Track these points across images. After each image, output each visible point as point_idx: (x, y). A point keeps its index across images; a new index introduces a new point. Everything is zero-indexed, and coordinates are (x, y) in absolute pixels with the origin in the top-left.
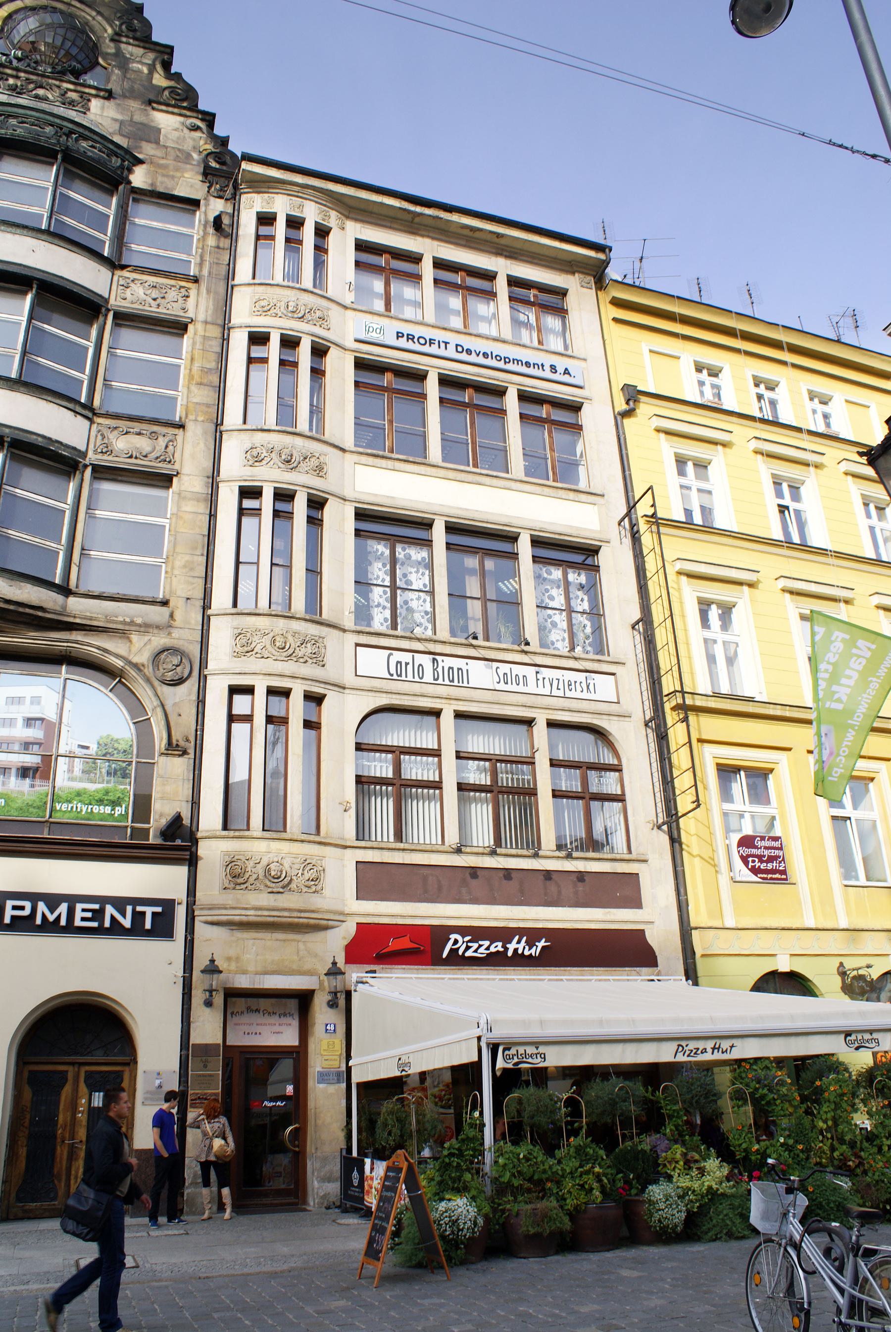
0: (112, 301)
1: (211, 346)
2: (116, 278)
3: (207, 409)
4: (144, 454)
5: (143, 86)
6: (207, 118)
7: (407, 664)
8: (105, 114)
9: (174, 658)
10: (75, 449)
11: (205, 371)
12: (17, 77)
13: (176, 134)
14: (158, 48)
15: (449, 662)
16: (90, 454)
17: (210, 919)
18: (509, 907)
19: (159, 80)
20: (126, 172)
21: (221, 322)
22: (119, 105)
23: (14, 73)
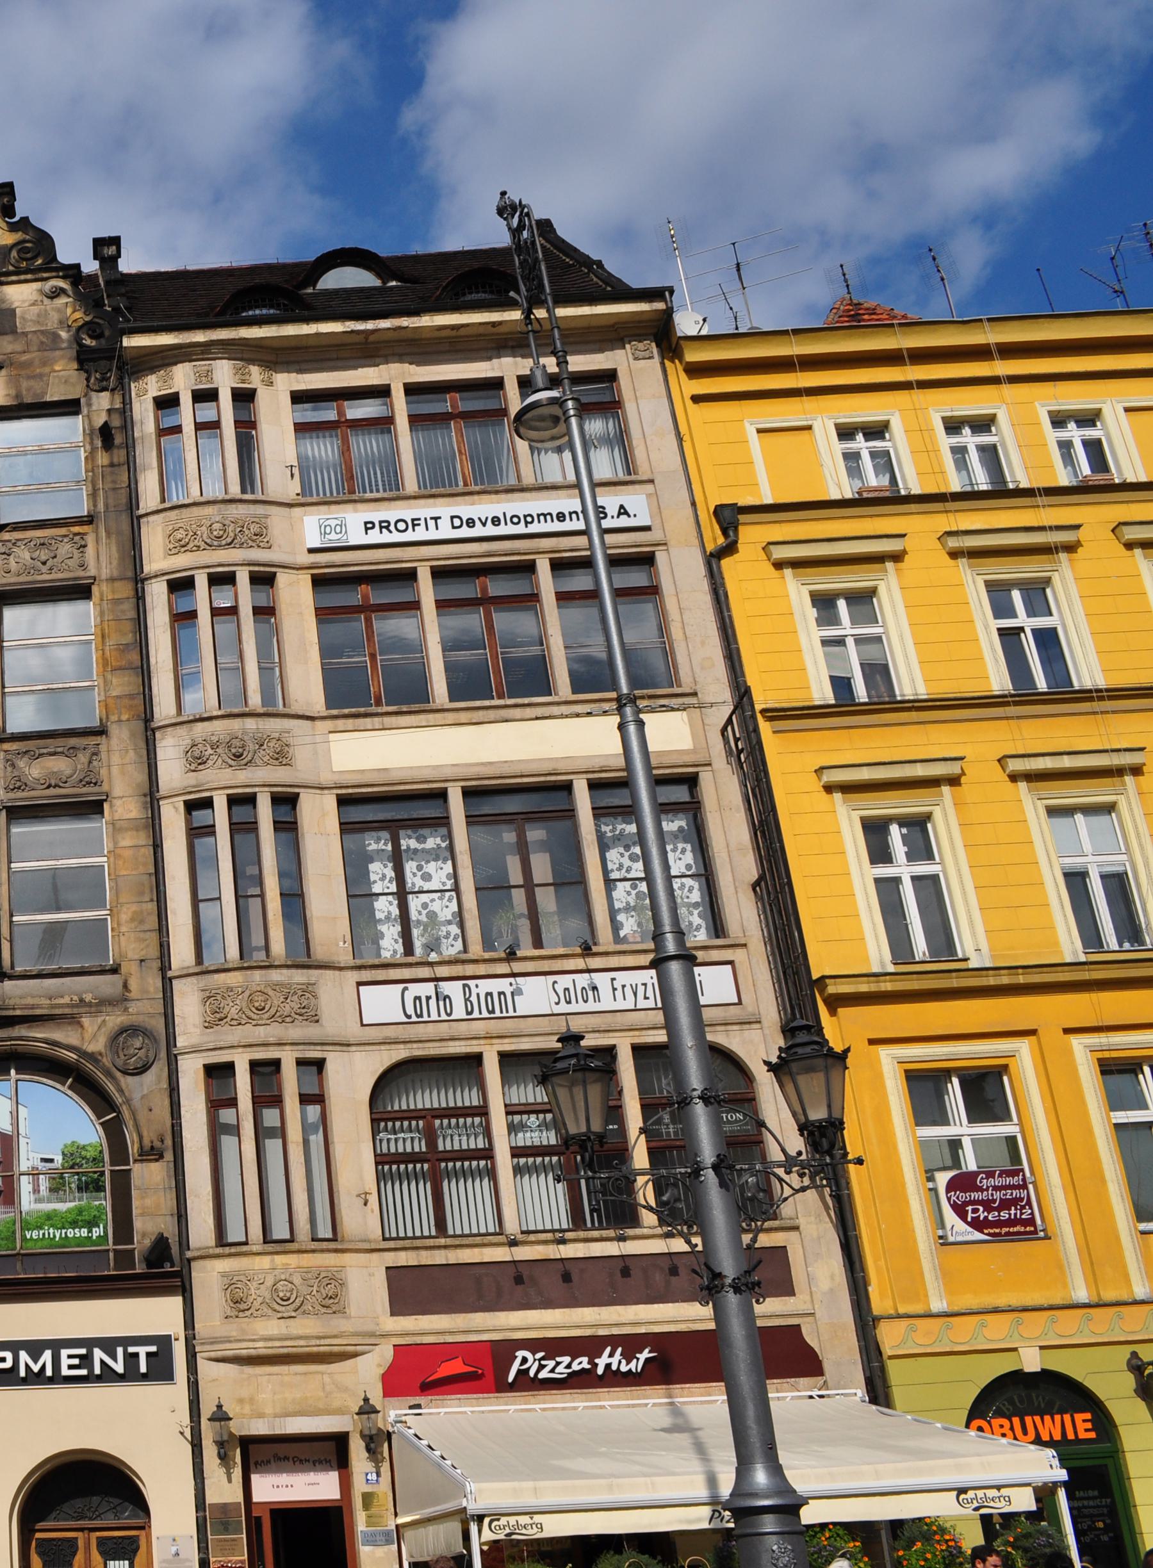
1: (123, 612)
3: (131, 702)
4: (64, 779)
6: (71, 272)
7: (428, 998)
9: (135, 1040)
11: (123, 649)
15: (486, 986)
17: (213, 1355)
18: (596, 1309)
21: (130, 574)
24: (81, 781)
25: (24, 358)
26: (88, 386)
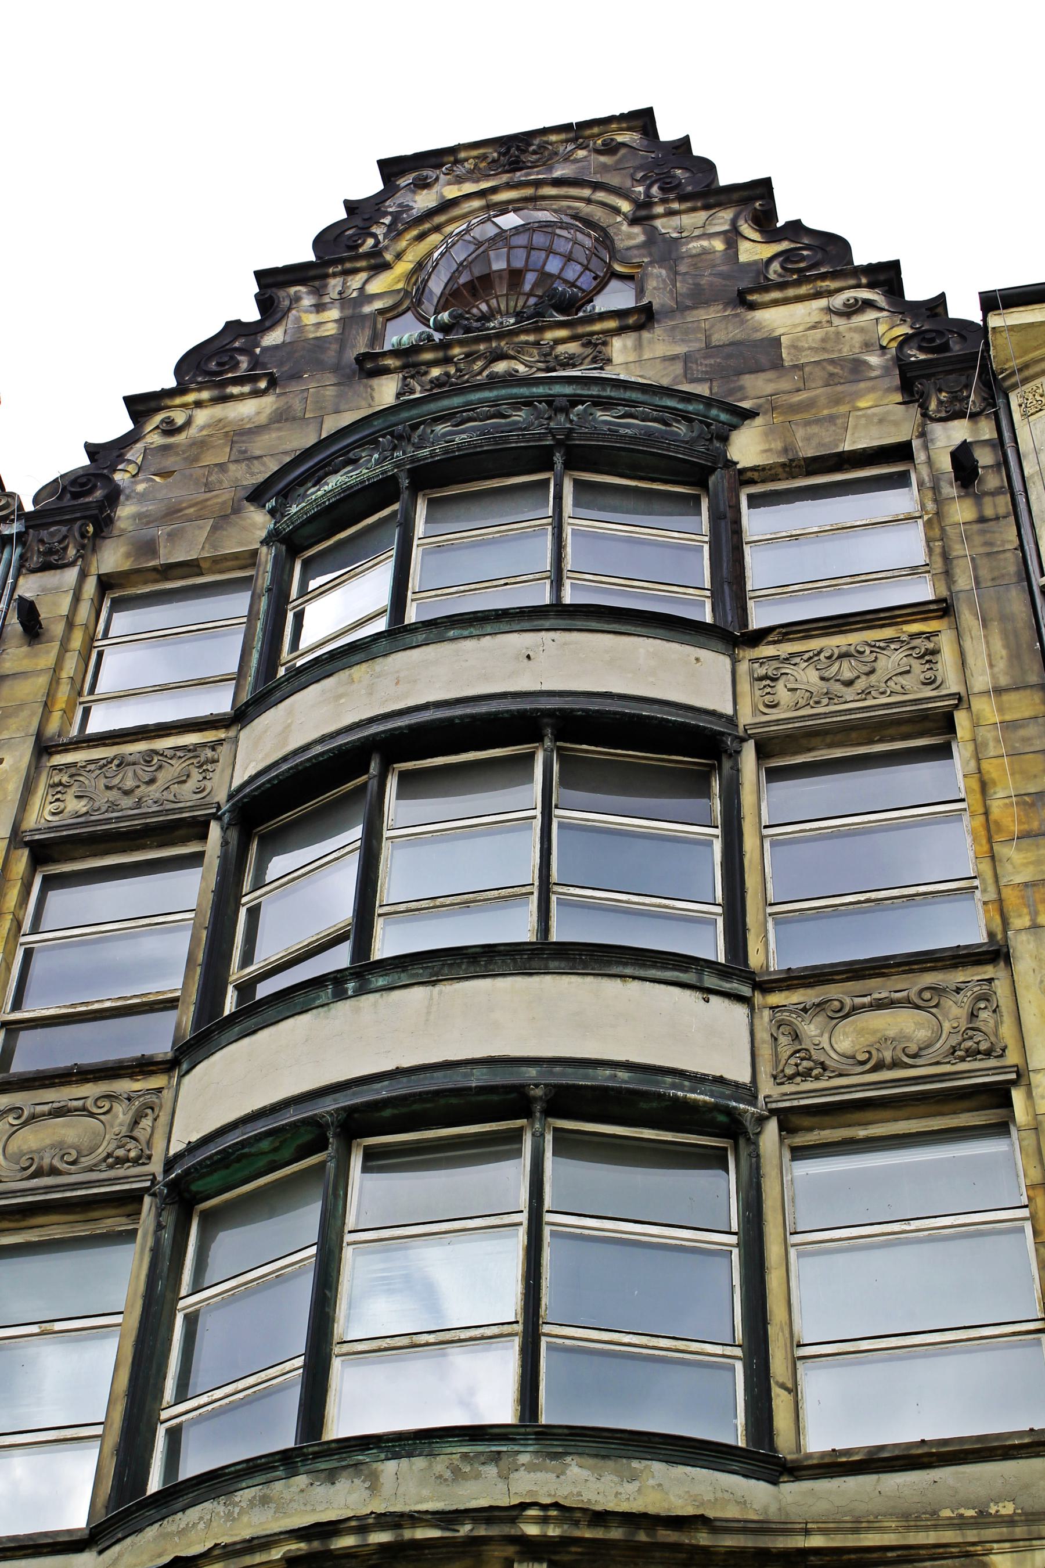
0: (746, 717)
1: (1025, 740)
2: (743, 667)
4: (913, 1048)
5: (720, 275)
6: (882, 277)
8: (645, 357)
10: (720, 1080)
12: (447, 360)
13: (819, 334)
14: (735, 196)
16: (767, 1088)
19: (754, 250)
20: (717, 444)
22: (674, 328)
23: (440, 355)
24: (954, 1050)
26: (925, 415)
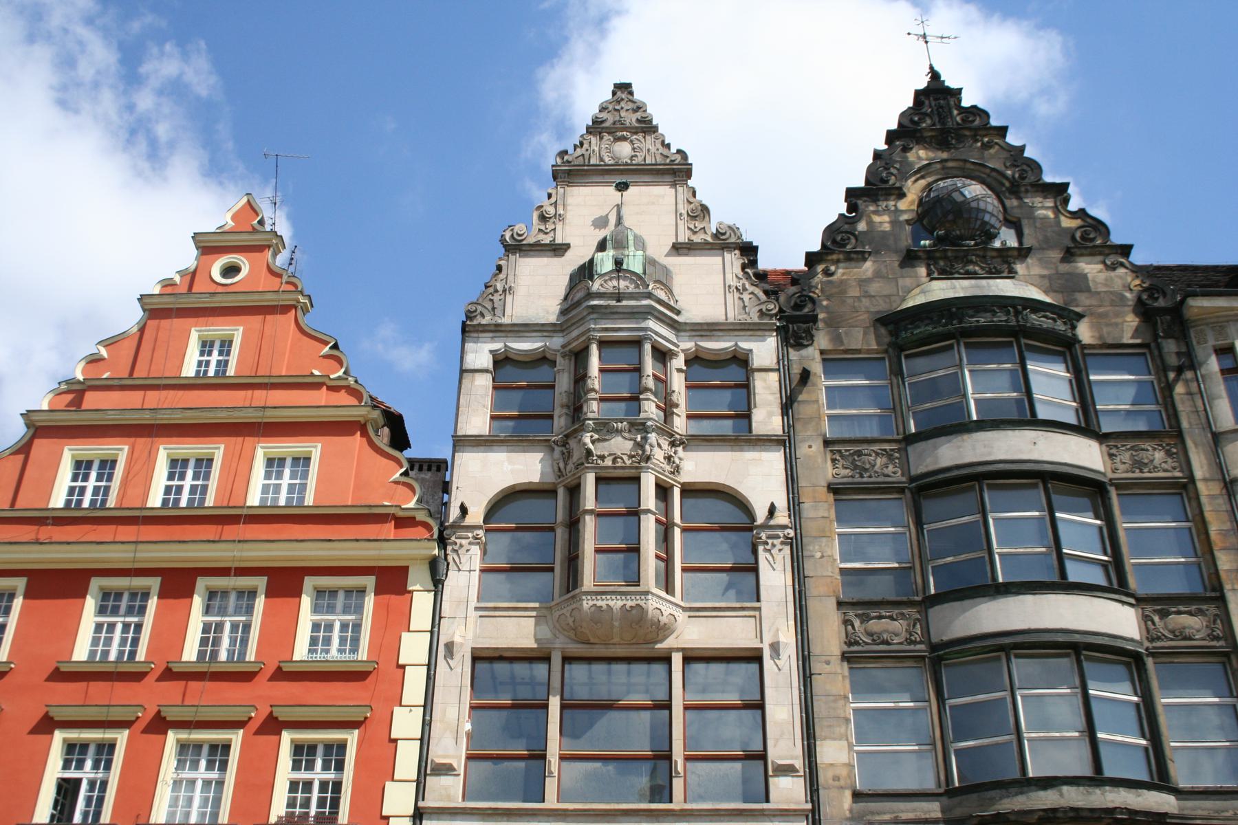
25: (1101, 310)
